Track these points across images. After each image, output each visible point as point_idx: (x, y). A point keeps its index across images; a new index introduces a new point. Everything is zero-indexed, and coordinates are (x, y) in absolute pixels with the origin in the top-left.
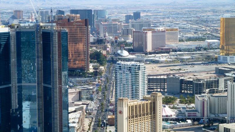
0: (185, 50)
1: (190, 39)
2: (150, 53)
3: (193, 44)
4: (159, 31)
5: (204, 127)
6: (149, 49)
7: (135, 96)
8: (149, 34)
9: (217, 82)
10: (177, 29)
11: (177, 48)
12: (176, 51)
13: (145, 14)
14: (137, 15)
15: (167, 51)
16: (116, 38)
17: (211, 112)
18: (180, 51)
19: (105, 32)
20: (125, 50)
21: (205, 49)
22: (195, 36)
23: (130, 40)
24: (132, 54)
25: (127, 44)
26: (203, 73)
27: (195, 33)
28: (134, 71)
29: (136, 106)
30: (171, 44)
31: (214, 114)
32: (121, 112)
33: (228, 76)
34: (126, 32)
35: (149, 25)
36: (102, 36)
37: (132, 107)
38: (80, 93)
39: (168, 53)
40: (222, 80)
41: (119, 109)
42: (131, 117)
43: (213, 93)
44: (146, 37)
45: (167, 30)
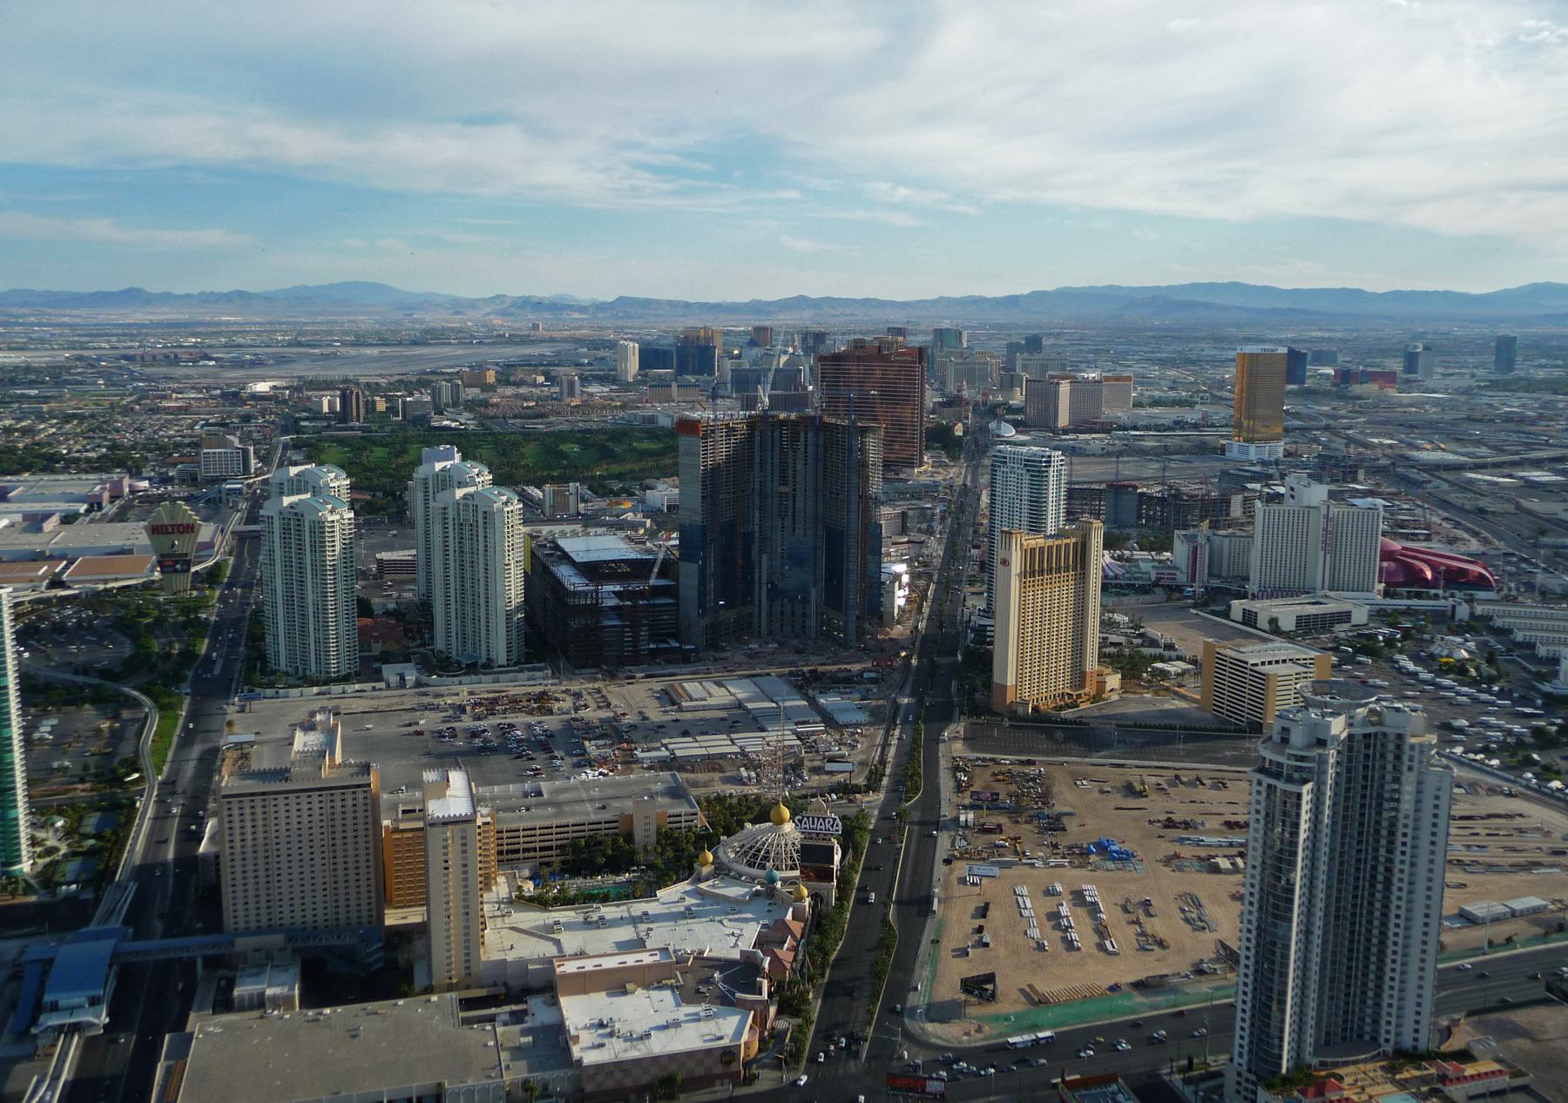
0: (1148, 428)
1: (1156, 403)
2: (1066, 432)
3: (1167, 415)
4: (1086, 381)
5: (1195, 606)
6: (1063, 420)
7: (1036, 525)
8: (1065, 388)
9: (1225, 502)
10: (1128, 378)
11: (1128, 422)
12: (1125, 429)
13: (1052, 341)
14: (1034, 344)
15: (1106, 428)
16: (984, 394)
17: (1211, 574)
18: (1135, 428)
19: (958, 379)
20: (1007, 421)
21: (1195, 426)
22: (1172, 394)
23: (1018, 398)
24: (1021, 433)
25: (1011, 410)
26: (1192, 481)
27: (1171, 389)
28: (1036, 470)
29: (1041, 549)
30: (1112, 412)
31: (1219, 577)
32: (1005, 562)
33: (1254, 491)
34: (1010, 382)
35: (1063, 367)
36: (951, 389)
37: (1033, 550)
38: (904, 515)
39: (1108, 431)
40: (1237, 501)
41: (1000, 554)
42: (1029, 573)
43: (1217, 528)
44: (1056, 394)
45: (1107, 379)
